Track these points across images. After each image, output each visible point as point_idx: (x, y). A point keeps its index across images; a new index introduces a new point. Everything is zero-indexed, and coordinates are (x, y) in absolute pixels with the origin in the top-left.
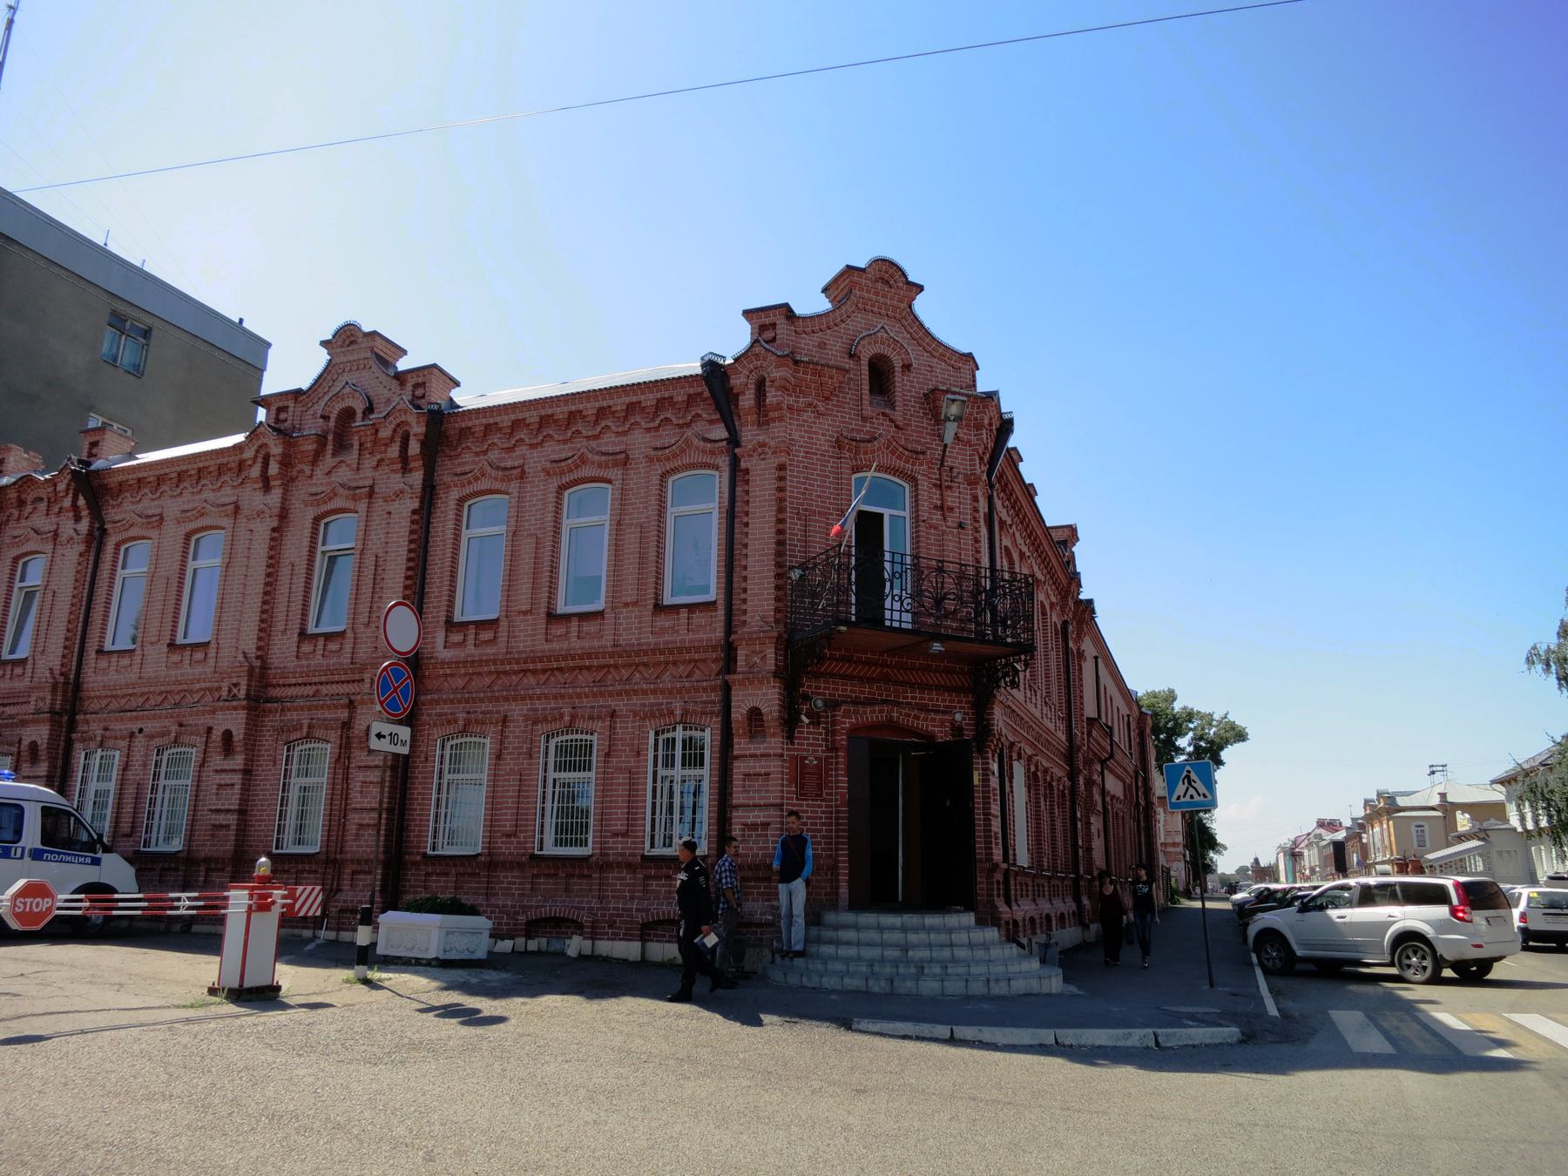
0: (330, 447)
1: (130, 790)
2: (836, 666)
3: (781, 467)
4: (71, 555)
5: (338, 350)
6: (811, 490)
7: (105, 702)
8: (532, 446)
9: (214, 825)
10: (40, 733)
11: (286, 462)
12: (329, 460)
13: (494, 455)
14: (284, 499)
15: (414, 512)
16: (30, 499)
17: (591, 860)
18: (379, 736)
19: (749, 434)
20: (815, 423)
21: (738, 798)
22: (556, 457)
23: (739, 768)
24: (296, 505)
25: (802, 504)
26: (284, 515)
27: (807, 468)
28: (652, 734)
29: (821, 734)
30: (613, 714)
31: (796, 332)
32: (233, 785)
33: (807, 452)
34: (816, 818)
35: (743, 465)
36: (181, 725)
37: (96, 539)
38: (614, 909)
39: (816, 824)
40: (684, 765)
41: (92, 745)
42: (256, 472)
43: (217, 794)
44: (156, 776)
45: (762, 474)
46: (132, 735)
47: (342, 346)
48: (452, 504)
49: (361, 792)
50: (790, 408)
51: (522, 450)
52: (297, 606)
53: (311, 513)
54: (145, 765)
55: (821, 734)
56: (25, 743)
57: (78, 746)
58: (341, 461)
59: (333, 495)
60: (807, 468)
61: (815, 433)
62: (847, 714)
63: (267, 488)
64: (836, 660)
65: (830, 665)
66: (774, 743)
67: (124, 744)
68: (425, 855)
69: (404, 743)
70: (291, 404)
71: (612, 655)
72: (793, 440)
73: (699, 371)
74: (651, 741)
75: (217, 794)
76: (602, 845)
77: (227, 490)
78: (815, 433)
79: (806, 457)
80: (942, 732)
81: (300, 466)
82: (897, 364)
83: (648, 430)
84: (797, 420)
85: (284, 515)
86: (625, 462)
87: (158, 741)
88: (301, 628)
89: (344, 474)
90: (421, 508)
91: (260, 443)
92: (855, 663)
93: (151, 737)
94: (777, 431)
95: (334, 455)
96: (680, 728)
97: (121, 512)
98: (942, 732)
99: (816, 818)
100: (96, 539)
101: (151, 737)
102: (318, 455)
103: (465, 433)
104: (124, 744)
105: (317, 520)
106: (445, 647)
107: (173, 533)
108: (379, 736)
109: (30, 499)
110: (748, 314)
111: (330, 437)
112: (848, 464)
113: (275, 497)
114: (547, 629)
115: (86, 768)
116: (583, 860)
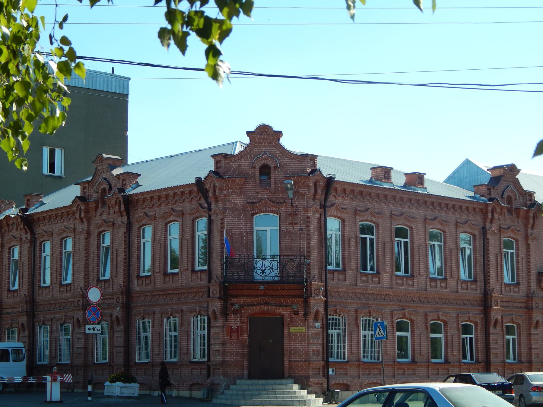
0: (100, 205)
1: (54, 341)
2: (245, 292)
3: (222, 219)
4: (26, 247)
5: (98, 164)
6: (236, 226)
7: (43, 307)
8: (158, 207)
9: (77, 353)
10: (23, 319)
11: (87, 211)
12: (100, 211)
13: (147, 210)
14: (88, 226)
15: (125, 233)
16: (11, 224)
17: (178, 363)
18: (89, 329)
19: (213, 206)
20: (236, 199)
21: (212, 342)
22: (164, 211)
23: (212, 330)
24: (92, 228)
25: (231, 232)
26: (88, 232)
27: (233, 217)
28: (192, 318)
29: (239, 317)
30: (182, 311)
31: (228, 163)
32: (81, 338)
33: (233, 211)
34: (237, 347)
35: (212, 218)
36: (66, 316)
37: (33, 241)
38: (184, 380)
39: (237, 349)
40: (200, 329)
41: (41, 323)
42: (77, 215)
43: (78, 342)
44: (61, 335)
45: (217, 220)
46: (52, 320)
47: (99, 163)
48: (136, 230)
49: (117, 340)
50: (225, 195)
51: (155, 208)
52: (95, 269)
53: (96, 232)
54: (57, 331)
55: (239, 317)
56: (20, 323)
57: (37, 324)
58: (104, 211)
59: (102, 225)
60: (233, 217)
61: (237, 203)
62: (246, 310)
63: (82, 222)
64: (245, 290)
65: (243, 292)
66: (220, 322)
67: (50, 323)
68: (135, 363)
69: (98, 330)
70: (87, 185)
71: (182, 289)
72: (227, 207)
73: (195, 182)
74: (192, 321)
75: (78, 342)
76: (181, 358)
77: (71, 222)
78: (237, 203)
79: (233, 213)
80: (287, 314)
81: (92, 212)
82: (272, 167)
83: (189, 202)
84: (229, 199)
85: (88, 232)
86: (183, 214)
87: (59, 322)
88: (97, 278)
89: (105, 216)
90: (127, 231)
91: (77, 204)
92: (253, 290)
93: (57, 320)
94: (220, 205)
95: (101, 207)
96: (199, 316)
97: (40, 230)
98: (287, 314)
99: (237, 347)
100: (33, 241)
101: (57, 320)
102: (96, 209)
103: (138, 201)
104: (50, 323)
105: (99, 234)
106: (137, 286)
107: (57, 238)
108: (89, 329)
109: (11, 224)
110: (212, 156)
111: (100, 201)
112: (250, 213)
113: (85, 226)
114: (164, 279)
115: (40, 333)
116: (175, 363)
